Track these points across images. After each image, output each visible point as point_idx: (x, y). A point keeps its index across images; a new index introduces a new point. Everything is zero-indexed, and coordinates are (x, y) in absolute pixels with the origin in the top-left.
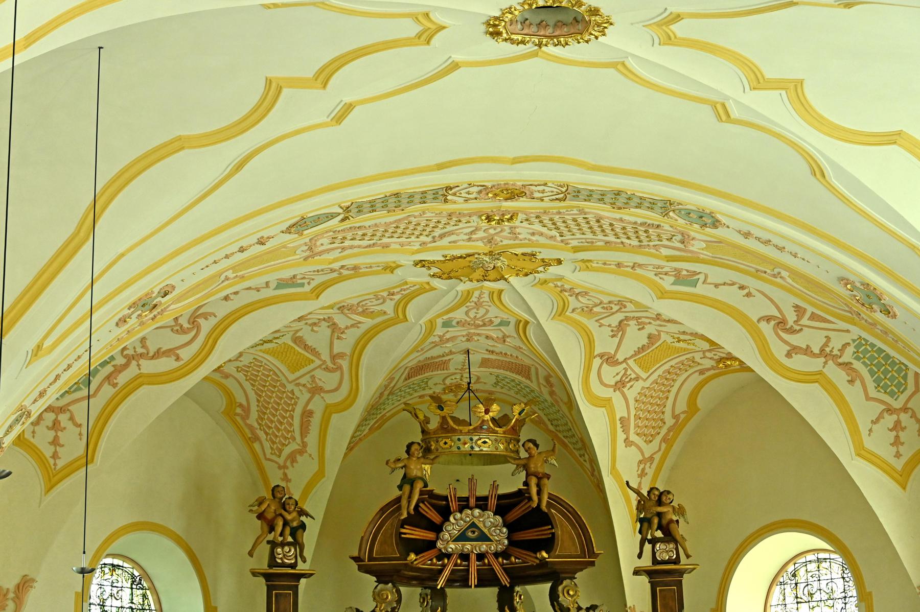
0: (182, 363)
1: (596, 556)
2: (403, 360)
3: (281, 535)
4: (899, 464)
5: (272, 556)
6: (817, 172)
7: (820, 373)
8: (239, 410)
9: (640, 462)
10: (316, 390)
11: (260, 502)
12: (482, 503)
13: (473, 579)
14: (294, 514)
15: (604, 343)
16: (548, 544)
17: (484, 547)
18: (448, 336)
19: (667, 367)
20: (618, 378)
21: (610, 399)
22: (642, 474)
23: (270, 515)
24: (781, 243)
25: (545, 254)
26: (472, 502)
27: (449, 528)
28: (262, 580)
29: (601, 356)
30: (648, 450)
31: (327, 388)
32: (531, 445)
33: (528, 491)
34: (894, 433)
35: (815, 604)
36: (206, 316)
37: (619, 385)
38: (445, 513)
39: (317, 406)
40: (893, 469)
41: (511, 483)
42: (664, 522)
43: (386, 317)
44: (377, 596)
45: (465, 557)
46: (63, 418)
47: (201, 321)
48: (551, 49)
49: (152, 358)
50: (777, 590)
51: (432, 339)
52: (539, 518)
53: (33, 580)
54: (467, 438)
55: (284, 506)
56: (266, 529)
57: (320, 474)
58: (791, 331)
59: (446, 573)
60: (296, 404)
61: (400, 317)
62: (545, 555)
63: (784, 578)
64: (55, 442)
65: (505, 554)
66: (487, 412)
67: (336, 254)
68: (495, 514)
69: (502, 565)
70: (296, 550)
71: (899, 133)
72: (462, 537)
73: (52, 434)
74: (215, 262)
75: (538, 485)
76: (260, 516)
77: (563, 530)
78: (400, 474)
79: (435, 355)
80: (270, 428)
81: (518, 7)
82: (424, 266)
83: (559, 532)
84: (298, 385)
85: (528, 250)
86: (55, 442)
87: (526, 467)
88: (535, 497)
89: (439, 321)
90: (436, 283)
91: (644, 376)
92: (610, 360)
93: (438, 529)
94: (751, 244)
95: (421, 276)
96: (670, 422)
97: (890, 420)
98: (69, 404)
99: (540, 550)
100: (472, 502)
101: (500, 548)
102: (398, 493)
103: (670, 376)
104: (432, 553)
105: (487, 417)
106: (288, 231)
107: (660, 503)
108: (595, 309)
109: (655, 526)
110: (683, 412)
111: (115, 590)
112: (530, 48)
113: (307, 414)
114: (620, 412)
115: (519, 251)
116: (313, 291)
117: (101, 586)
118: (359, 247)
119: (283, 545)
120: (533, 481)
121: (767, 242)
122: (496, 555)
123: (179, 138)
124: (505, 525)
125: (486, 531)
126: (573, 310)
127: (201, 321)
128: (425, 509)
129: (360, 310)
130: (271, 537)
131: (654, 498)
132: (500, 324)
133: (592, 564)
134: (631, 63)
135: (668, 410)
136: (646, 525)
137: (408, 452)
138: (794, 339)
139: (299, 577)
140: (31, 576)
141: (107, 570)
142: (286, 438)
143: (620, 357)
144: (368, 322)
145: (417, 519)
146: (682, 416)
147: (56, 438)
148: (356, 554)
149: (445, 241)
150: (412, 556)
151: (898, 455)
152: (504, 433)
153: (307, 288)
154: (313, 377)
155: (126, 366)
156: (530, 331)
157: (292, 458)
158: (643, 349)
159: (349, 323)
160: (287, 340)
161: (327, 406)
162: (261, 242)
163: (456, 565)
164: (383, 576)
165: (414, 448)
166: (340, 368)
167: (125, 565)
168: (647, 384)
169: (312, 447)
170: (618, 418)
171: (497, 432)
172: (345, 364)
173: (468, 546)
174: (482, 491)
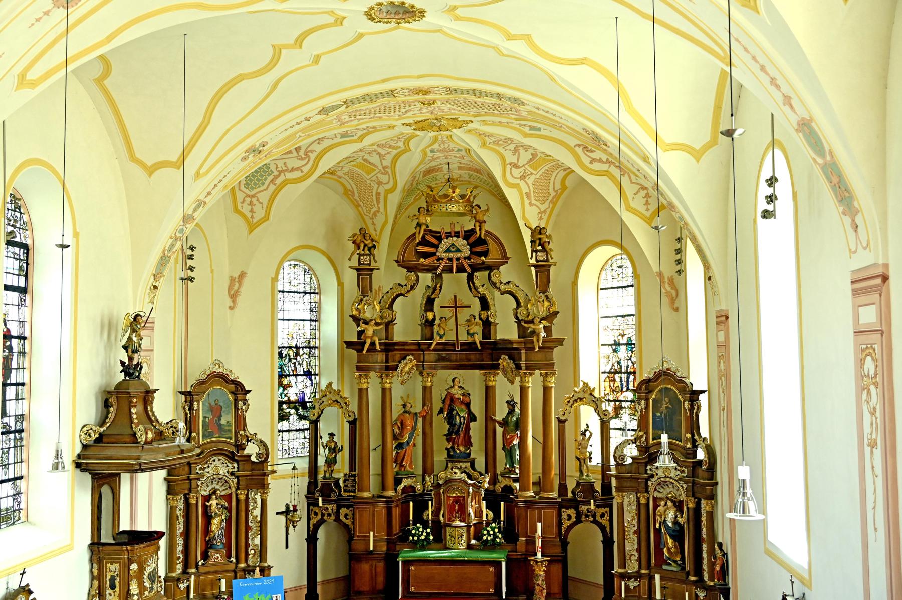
0: (303, 174)
1: (509, 259)
2: (416, 169)
3: (363, 250)
4: (648, 214)
5: (359, 261)
6: (552, 79)
7: (607, 171)
8: (350, 193)
9: (539, 213)
10: (380, 183)
11: (354, 236)
12: (457, 235)
13: (454, 270)
14: (369, 241)
15: (510, 158)
16: (485, 254)
17: (459, 255)
18: (435, 156)
19: (546, 168)
20: (521, 174)
21: (518, 184)
22: (541, 219)
23: (358, 242)
24: (554, 113)
25: (461, 118)
26: (453, 234)
27: (442, 246)
28: (355, 271)
29: (510, 164)
30: (543, 208)
31: (384, 182)
32: (476, 207)
33: (475, 229)
34: (646, 199)
35: (619, 279)
36: (311, 151)
37: (523, 178)
38: (440, 239)
39: (381, 190)
40: (646, 217)
41: (469, 226)
42: (542, 242)
43: (401, 149)
44: (407, 278)
45: (450, 260)
46: (254, 200)
47: (310, 154)
48: (403, 24)
49: (290, 171)
50: (604, 273)
51: (428, 158)
52: (481, 242)
53: (246, 273)
54: (445, 205)
55: (364, 237)
56: (356, 248)
57: (386, 222)
58: (592, 151)
59: (441, 267)
60: (373, 189)
61: (407, 150)
62: (483, 258)
63: (607, 267)
64: (252, 211)
65: (469, 258)
66: (453, 192)
67: (356, 122)
68: (463, 240)
69: (467, 263)
70: (370, 258)
71: (585, 58)
72: (448, 251)
73: (250, 207)
74: (286, 130)
75: (480, 226)
76: (354, 242)
77: (492, 246)
78: (416, 222)
79: (434, 165)
80: (364, 201)
81: (375, 6)
82: (407, 125)
83: (490, 248)
84: (372, 181)
85: (454, 117)
86: (252, 211)
87: (475, 218)
88: (478, 232)
89: (428, 150)
90: (418, 132)
91: (535, 173)
92: (515, 166)
93: (437, 247)
94: (540, 112)
95: (408, 130)
96: (553, 194)
97: (643, 193)
98: (255, 194)
99: (481, 257)
100: (453, 234)
101: (466, 255)
102: (414, 231)
103: (548, 173)
104: (434, 258)
105: (454, 195)
106: (319, 113)
107: (540, 233)
108: (500, 142)
109: (537, 245)
110: (560, 189)
111: (296, 276)
112: (393, 24)
113: (378, 194)
114: (525, 190)
115: (449, 117)
116: (359, 138)
117: (289, 274)
118: (366, 118)
119: (364, 255)
120: (477, 224)
121: (547, 112)
122: (465, 258)
123: (240, 75)
124: (468, 244)
125: (459, 248)
126: (490, 143)
127: (310, 154)
128: (428, 238)
129: (388, 146)
130: (358, 252)
131: (537, 231)
132: (458, 151)
133: (507, 262)
134: (445, 29)
135: (551, 188)
136: (533, 244)
137: (419, 212)
138: (593, 155)
139: (372, 270)
140: (245, 271)
141: (291, 267)
142: (371, 205)
143: (520, 164)
144: (394, 152)
145: (424, 242)
146: (559, 191)
147: (252, 209)
148: (396, 259)
149: (409, 114)
150: (422, 260)
151: (648, 210)
152: (463, 202)
153: (355, 138)
154: (377, 177)
155: (279, 175)
156: (472, 153)
157: (375, 214)
158: (530, 160)
159: (386, 152)
160: (360, 160)
161: (386, 191)
162: (307, 119)
163: (446, 263)
164: (410, 270)
165: (422, 209)
166: (387, 173)
167: (301, 264)
168: (538, 176)
169: (382, 210)
170: (524, 192)
171: (459, 202)
172: (390, 171)
173: (451, 255)
174: (457, 229)
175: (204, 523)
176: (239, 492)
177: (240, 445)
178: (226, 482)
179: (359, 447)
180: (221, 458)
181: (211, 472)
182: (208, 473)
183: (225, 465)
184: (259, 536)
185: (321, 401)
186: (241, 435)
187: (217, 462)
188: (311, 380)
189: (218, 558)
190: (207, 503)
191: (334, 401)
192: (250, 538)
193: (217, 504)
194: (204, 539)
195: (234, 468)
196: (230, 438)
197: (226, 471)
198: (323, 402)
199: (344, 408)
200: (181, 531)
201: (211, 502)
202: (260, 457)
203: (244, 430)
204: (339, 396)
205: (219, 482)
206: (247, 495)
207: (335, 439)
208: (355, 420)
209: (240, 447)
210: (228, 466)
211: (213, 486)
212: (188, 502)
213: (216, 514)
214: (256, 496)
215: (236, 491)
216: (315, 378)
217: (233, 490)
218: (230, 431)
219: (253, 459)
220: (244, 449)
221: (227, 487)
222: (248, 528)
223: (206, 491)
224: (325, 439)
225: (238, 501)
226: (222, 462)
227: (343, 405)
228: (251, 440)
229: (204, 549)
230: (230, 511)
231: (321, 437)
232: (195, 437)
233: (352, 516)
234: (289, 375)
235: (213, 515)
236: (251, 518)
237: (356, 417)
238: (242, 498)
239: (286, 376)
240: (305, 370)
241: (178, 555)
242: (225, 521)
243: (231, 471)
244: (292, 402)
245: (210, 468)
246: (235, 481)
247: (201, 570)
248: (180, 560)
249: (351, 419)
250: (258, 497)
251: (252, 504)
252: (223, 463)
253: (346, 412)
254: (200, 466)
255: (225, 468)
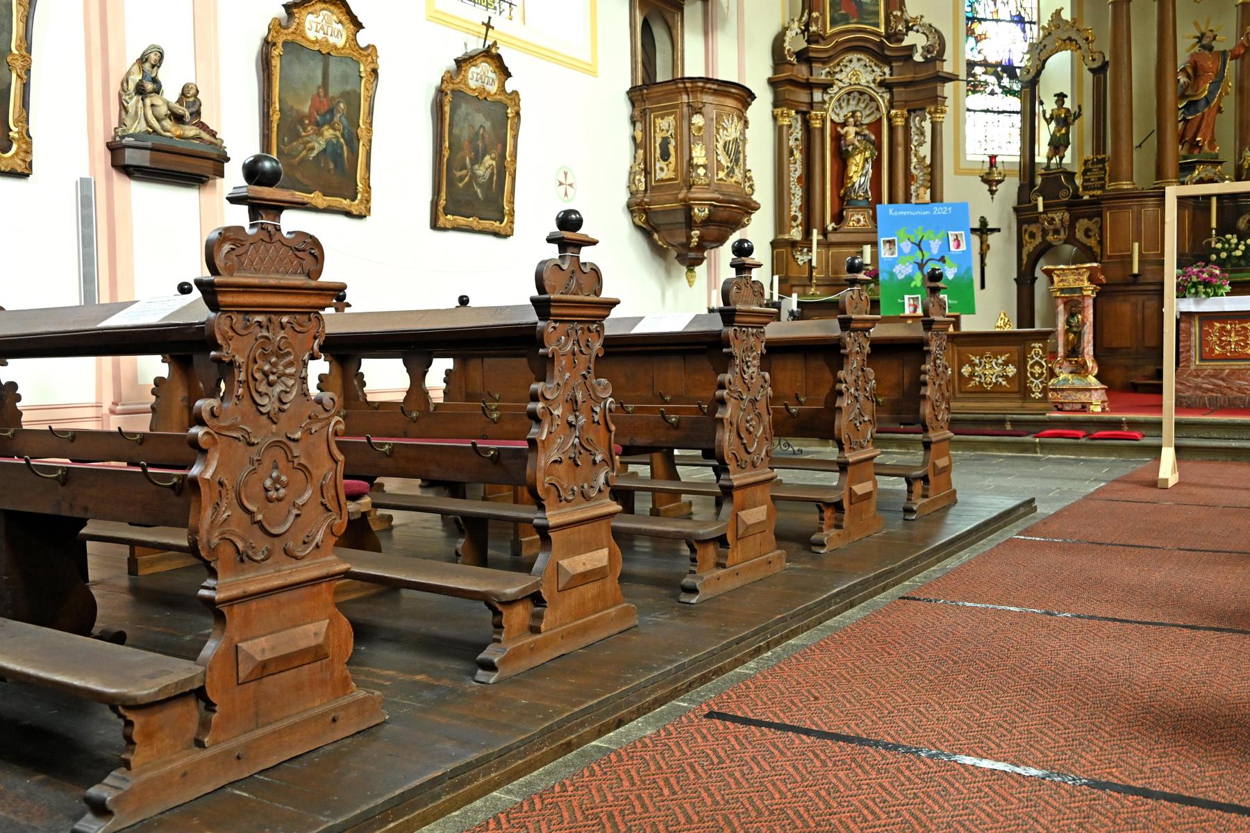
175: (836, 167)
176: (893, 112)
177: (895, 34)
178: (872, 99)
179: (1111, 83)
180: (862, 56)
181: (847, 80)
182: (841, 81)
183: (869, 69)
184: (929, 191)
185: (1041, 47)
186: (895, 17)
187: (855, 65)
188: (1024, 31)
189: (859, 221)
190: (839, 129)
191: (1065, 41)
192: (914, 194)
193: (857, 134)
194: (835, 193)
195: (884, 73)
196: (877, 25)
197: (870, 78)
198: (1045, 46)
199: (1083, 48)
200: (798, 173)
201: (846, 129)
202: (929, 52)
203: (902, 12)
204: (1075, 29)
205: (859, 99)
206: (907, 120)
207: (1068, 104)
208: (1105, 65)
209: (896, 37)
210: (873, 71)
211: (851, 108)
212: (809, 126)
213: (856, 148)
214: (923, 124)
215: (889, 112)
216: (1031, 29)
217: (884, 111)
218: (877, 13)
219: (918, 57)
220: (902, 40)
221: (874, 109)
222: (909, 178)
223: (838, 115)
224: (1050, 106)
225: (892, 129)
226: (863, 63)
227: (1082, 42)
228: (913, 25)
229: (837, 210)
230: (879, 149)
231: (1041, 103)
232: (817, 18)
233: (1097, 230)
234: (985, 20)
235: (850, 148)
236: (914, 160)
237: (1107, 59)
238: (899, 122)
239: (980, 20)
240: (1014, 14)
241: (793, 213)
242: (870, 160)
243: (879, 79)
244: (991, 65)
245: (844, 73)
246: (887, 96)
247: (833, 238)
248: (799, 221)
249: (1095, 65)
250: (927, 126)
251: (916, 137)
252: (865, 65)
253: (1085, 55)
254: (827, 69)
255: (868, 74)
